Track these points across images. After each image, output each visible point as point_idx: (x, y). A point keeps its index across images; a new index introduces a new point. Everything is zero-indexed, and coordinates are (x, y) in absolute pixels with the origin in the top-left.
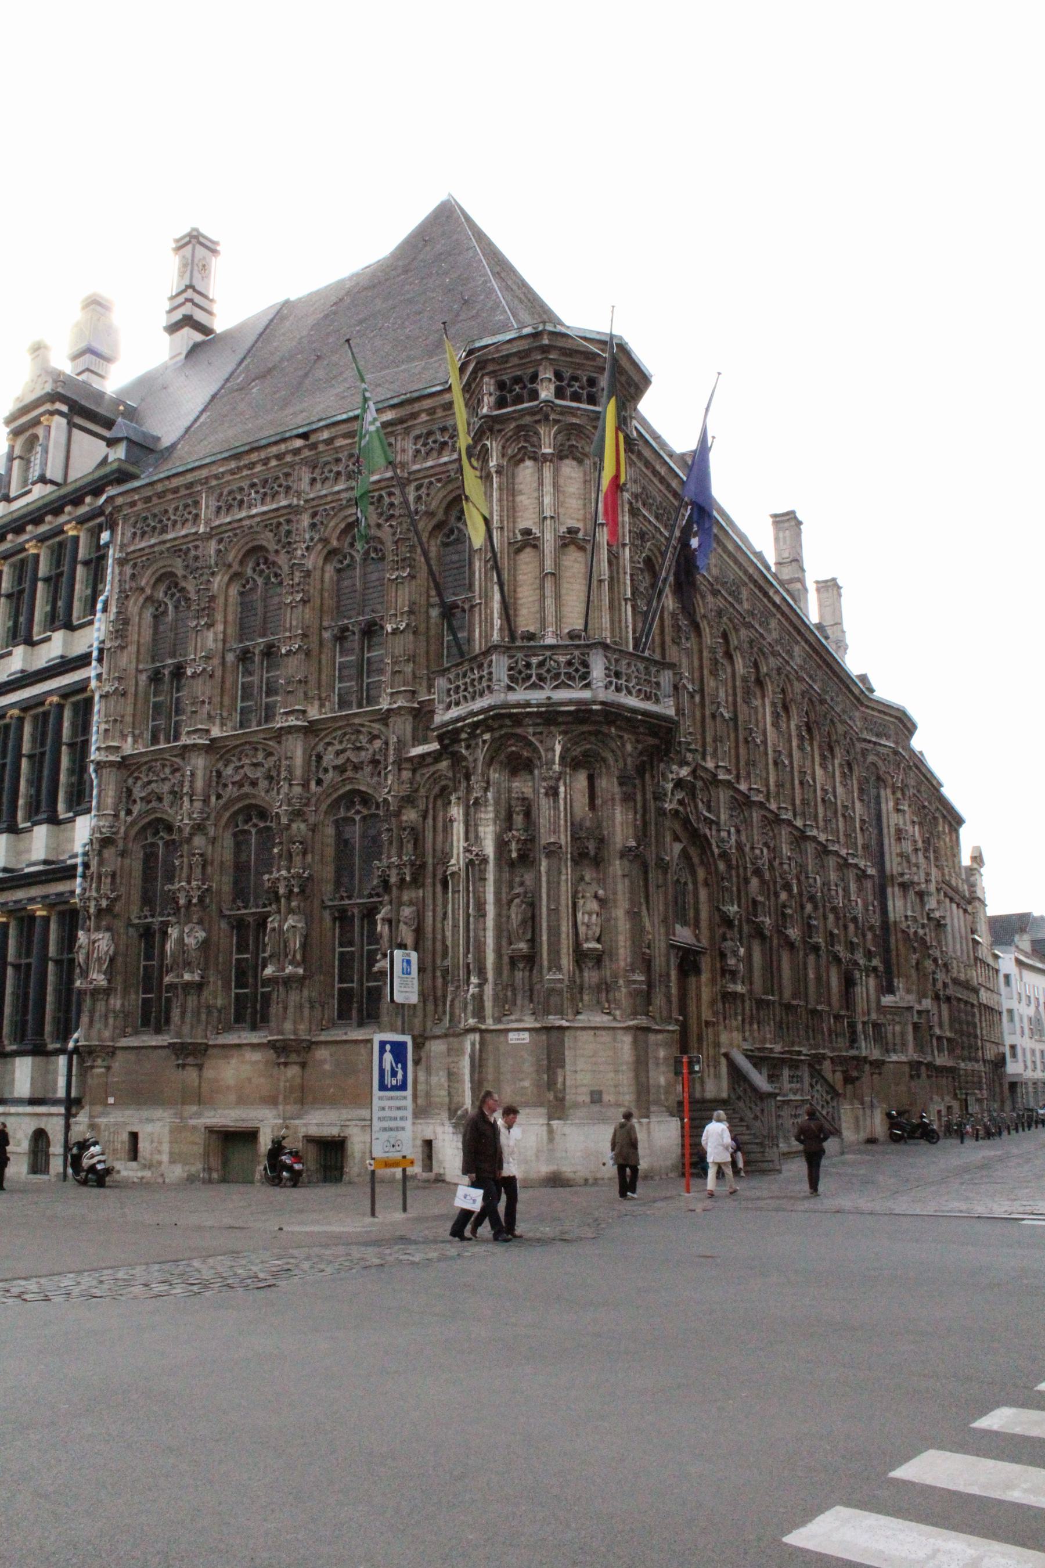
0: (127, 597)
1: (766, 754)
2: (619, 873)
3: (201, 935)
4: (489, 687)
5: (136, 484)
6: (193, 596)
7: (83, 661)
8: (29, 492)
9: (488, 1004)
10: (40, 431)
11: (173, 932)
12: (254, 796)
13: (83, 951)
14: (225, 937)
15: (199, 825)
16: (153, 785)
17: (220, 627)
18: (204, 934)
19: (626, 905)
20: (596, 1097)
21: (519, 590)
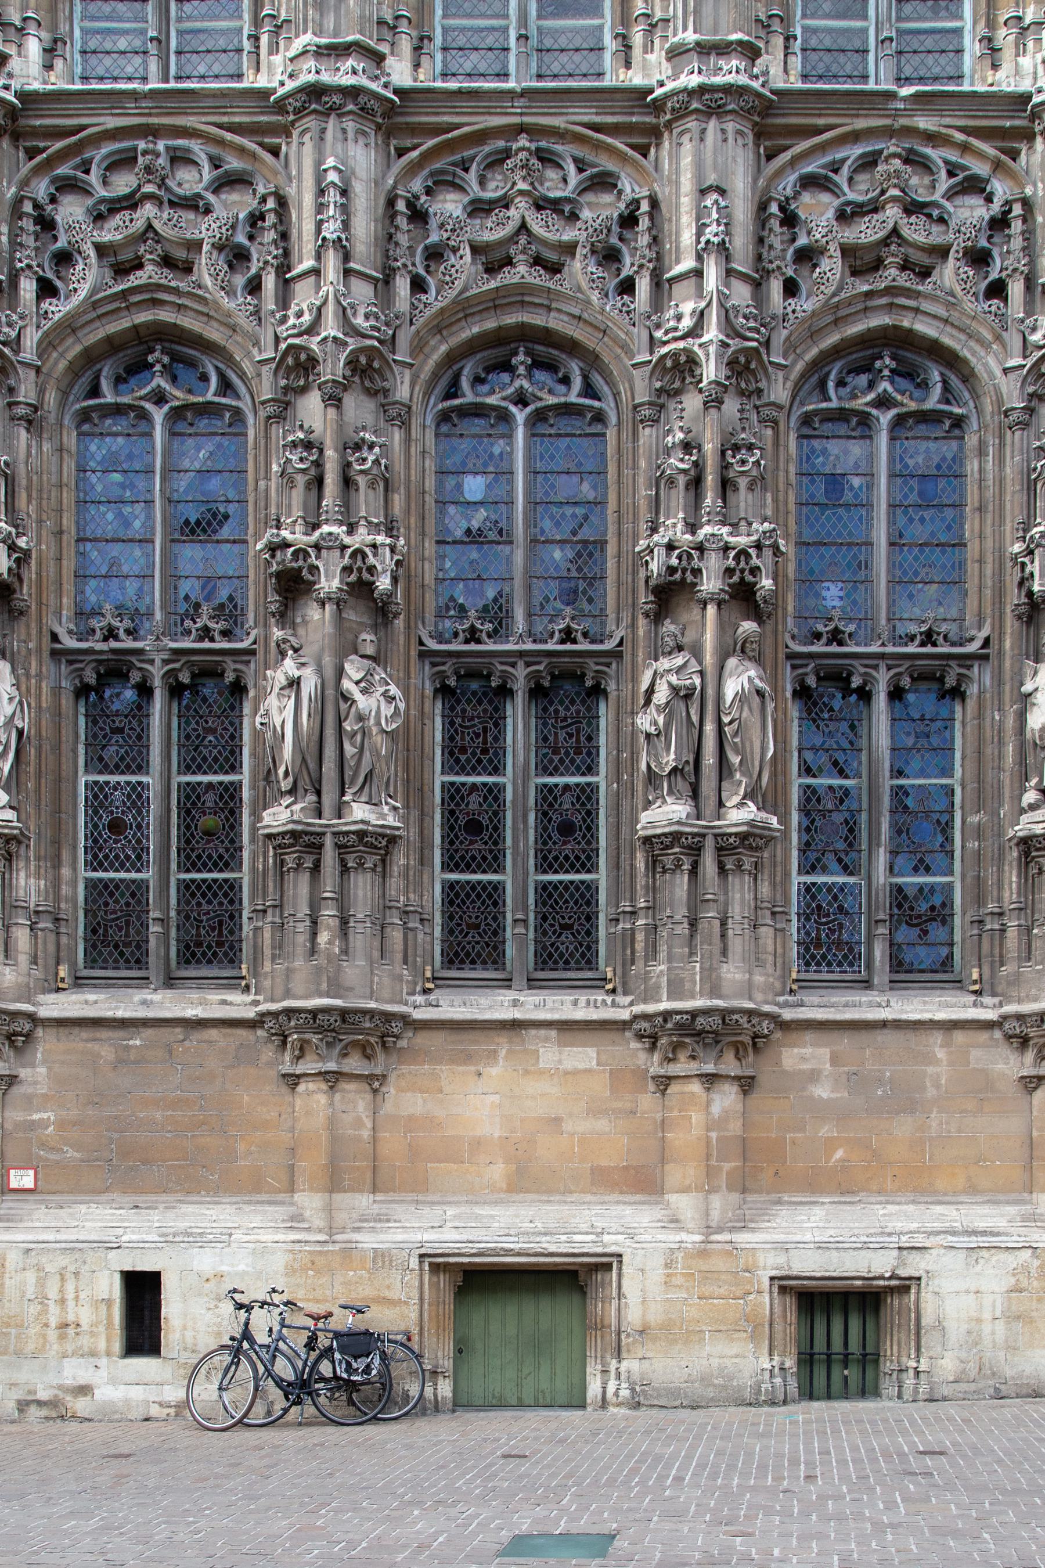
16: (148, 210)
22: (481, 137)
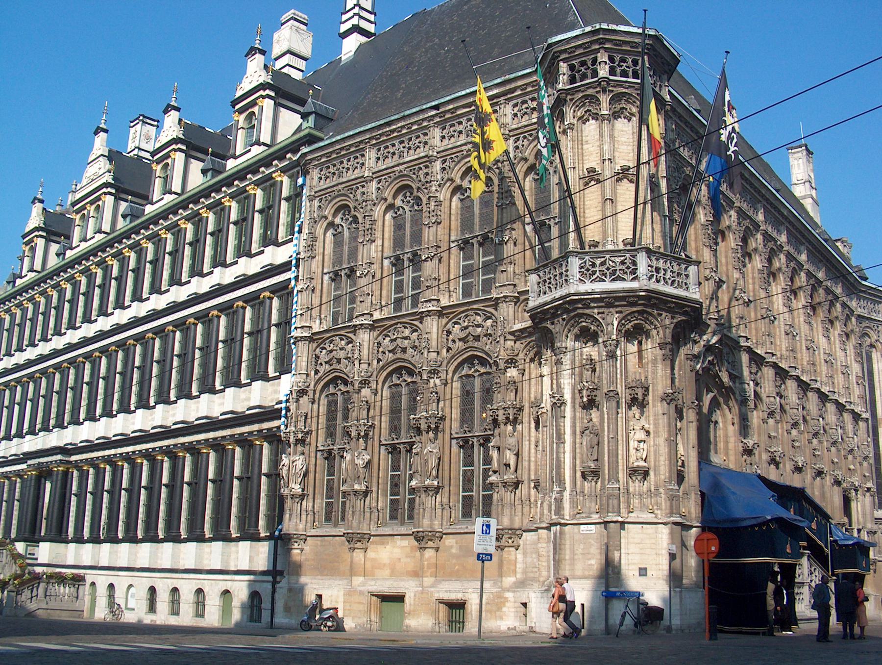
0: (315, 222)
1: (780, 327)
2: (661, 412)
3: (367, 457)
4: (566, 280)
5: (321, 144)
6: (361, 220)
7: (285, 267)
8: (250, 151)
9: (567, 505)
10: (256, 109)
11: (348, 456)
12: (404, 360)
13: (285, 468)
14: (385, 460)
15: (365, 380)
16: (334, 352)
17: (380, 242)
18: (368, 457)
19: (666, 435)
20: (643, 572)
21: (587, 211)
22: (391, 326)
